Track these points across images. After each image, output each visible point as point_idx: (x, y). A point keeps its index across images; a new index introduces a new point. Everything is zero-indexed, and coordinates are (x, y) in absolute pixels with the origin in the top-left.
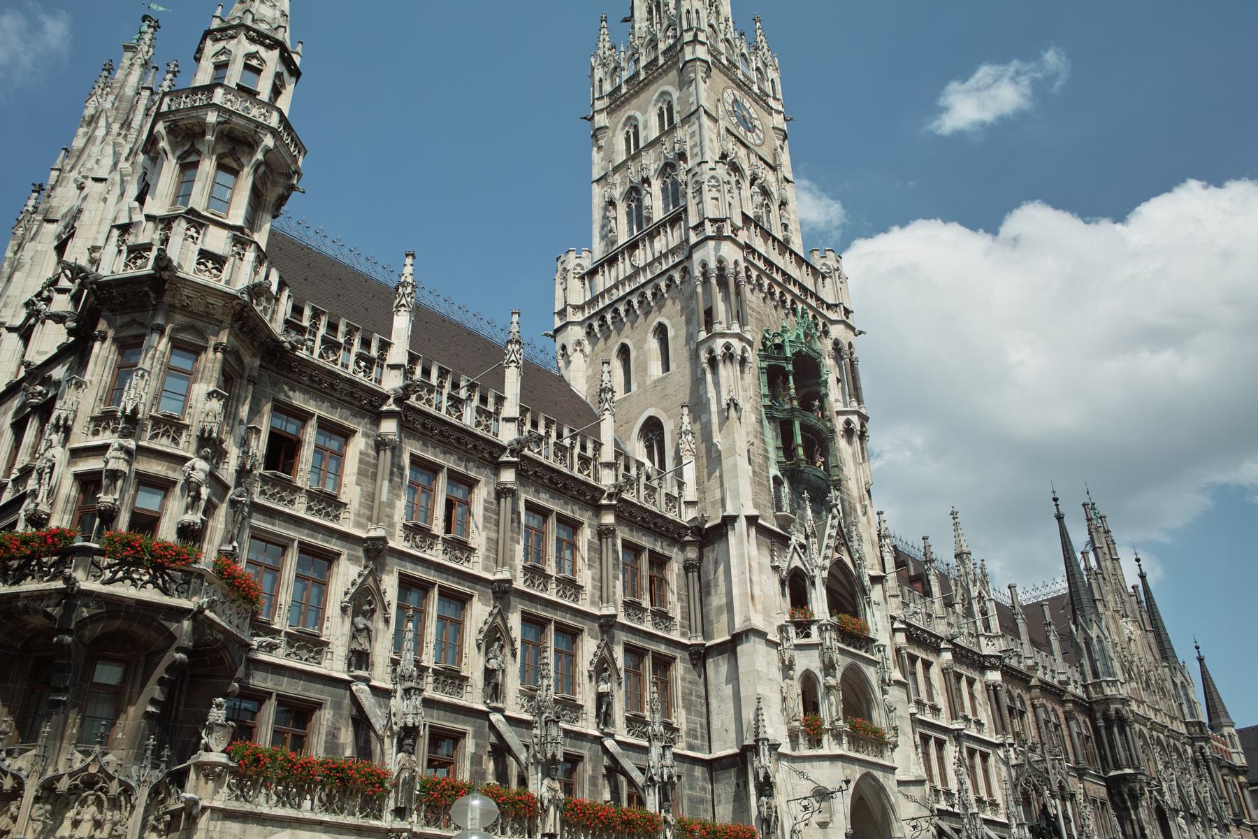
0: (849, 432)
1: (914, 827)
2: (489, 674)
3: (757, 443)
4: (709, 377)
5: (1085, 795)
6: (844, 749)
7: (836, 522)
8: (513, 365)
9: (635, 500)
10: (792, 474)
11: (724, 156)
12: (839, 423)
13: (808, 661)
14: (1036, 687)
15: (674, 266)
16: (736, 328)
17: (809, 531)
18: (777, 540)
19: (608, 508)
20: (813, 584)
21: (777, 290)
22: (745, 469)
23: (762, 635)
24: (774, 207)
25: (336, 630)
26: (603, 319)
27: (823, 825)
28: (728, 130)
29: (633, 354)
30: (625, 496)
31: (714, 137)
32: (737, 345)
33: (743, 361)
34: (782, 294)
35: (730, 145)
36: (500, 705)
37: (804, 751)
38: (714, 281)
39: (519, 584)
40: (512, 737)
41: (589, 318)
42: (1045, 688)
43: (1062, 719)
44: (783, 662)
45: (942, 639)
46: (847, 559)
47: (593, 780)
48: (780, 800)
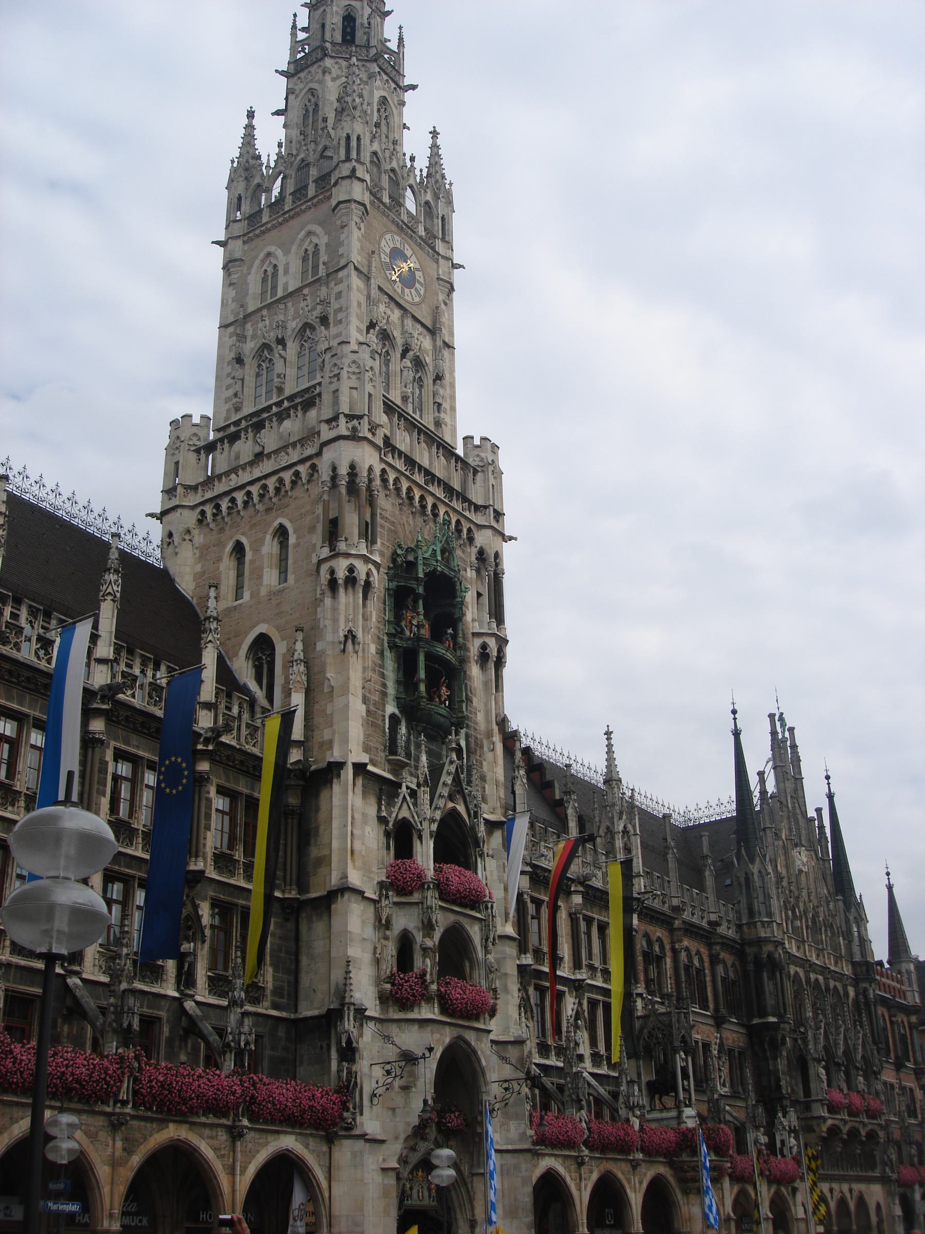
0: (484, 656)
1: (506, 1089)
3: (375, 677)
4: (328, 601)
5: (721, 1045)
7: (452, 769)
8: (109, 598)
9: (234, 743)
10: (410, 710)
11: (372, 326)
12: (474, 647)
13: (405, 920)
14: (679, 929)
15: (302, 461)
17: (421, 780)
18: (385, 790)
19: (205, 754)
20: (420, 837)
21: (417, 494)
22: (357, 708)
23: (361, 893)
24: (428, 381)
26: (217, 507)
27: (406, 1088)
28: (380, 289)
29: (249, 556)
30: (224, 739)
31: (363, 299)
32: (362, 569)
33: (368, 585)
34: (422, 498)
35: (382, 308)
36: (77, 968)
38: (343, 490)
40: (89, 1002)
41: (203, 503)
42: (691, 930)
43: (707, 964)
44: (380, 920)
45: (573, 881)
46: (461, 809)
47: (170, 1041)
48: (363, 1065)
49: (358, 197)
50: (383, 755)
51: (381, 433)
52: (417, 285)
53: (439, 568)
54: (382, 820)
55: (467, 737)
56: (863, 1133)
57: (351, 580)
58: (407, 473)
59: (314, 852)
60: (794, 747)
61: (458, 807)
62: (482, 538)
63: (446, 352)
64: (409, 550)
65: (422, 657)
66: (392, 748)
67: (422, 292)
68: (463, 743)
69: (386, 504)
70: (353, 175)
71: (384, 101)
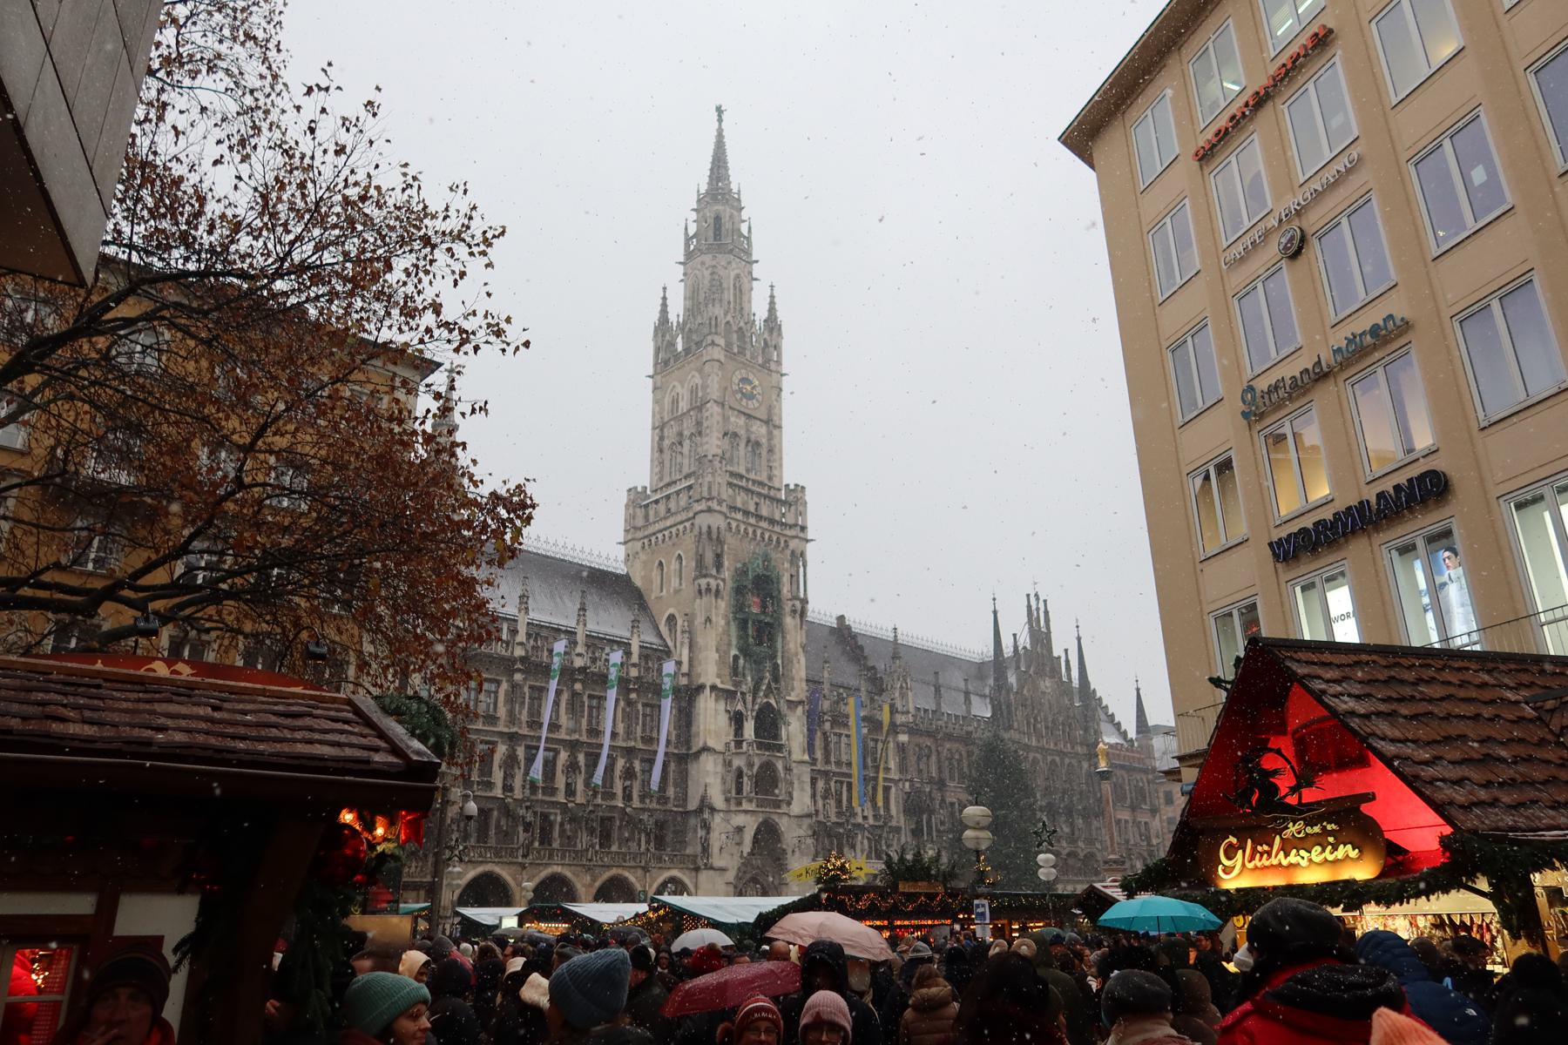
0: (794, 612)
2: (568, 785)
6: (752, 807)
10: (745, 651)
11: (725, 434)
12: (787, 607)
13: (738, 762)
16: (714, 572)
18: (729, 695)
19: (634, 690)
21: (750, 530)
25: (498, 776)
32: (713, 583)
33: (718, 591)
37: (733, 808)
39: (584, 738)
49: (716, 357)
56: (1082, 855)
57: (708, 590)
59: (694, 729)
60: (1046, 613)
62: (793, 544)
63: (776, 432)
66: (735, 671)
69: (731, 541)
70: (713, 343)
71: (738, 277)
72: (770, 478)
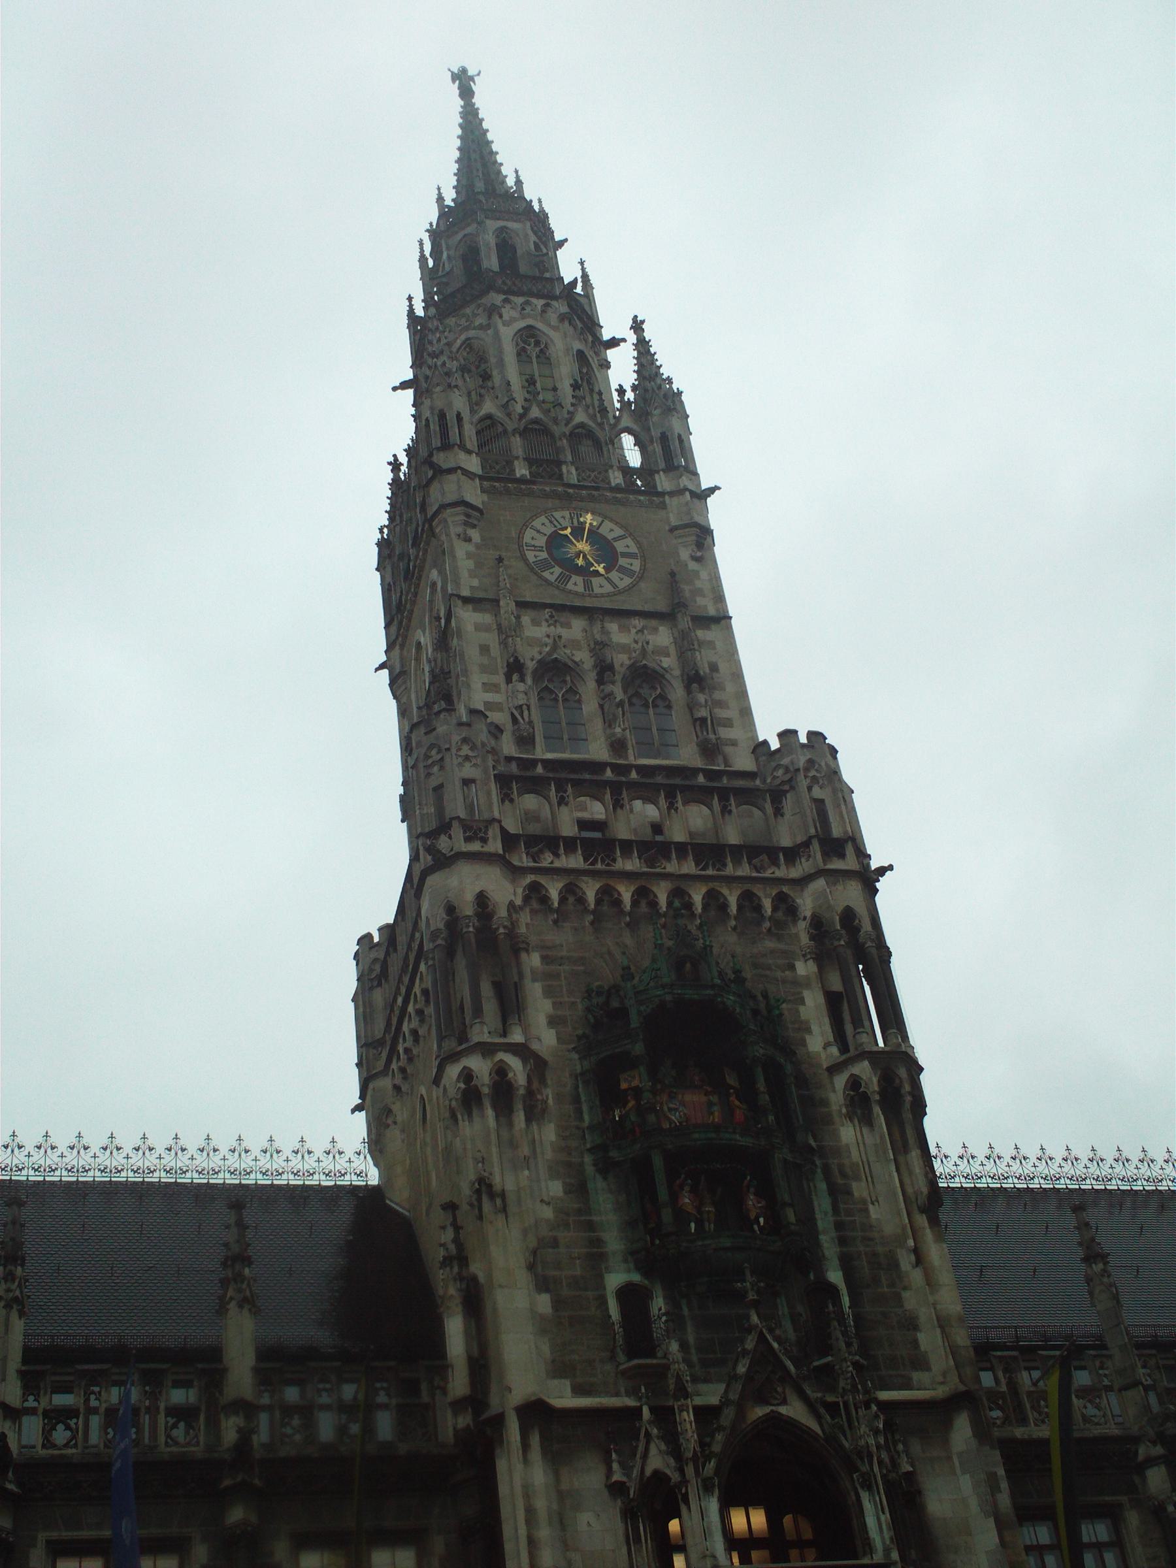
11: (515, 668)
12: (836, 1093)
24: (677, 693)
46: (794, 1410)
49: (451, 498)
50: (608, 1367)
51: (494, 832)
52: (622, 561)
53: (668, 998)
54: (616, 1489)
55: (847, 1264)
58: (599, 866)
61: (783, 1410)
64: (615, 989)
65: (658, 1162)
67: (636, 565)
68: (835, 1276)
71: (528, 335)
72: (710, 750)
